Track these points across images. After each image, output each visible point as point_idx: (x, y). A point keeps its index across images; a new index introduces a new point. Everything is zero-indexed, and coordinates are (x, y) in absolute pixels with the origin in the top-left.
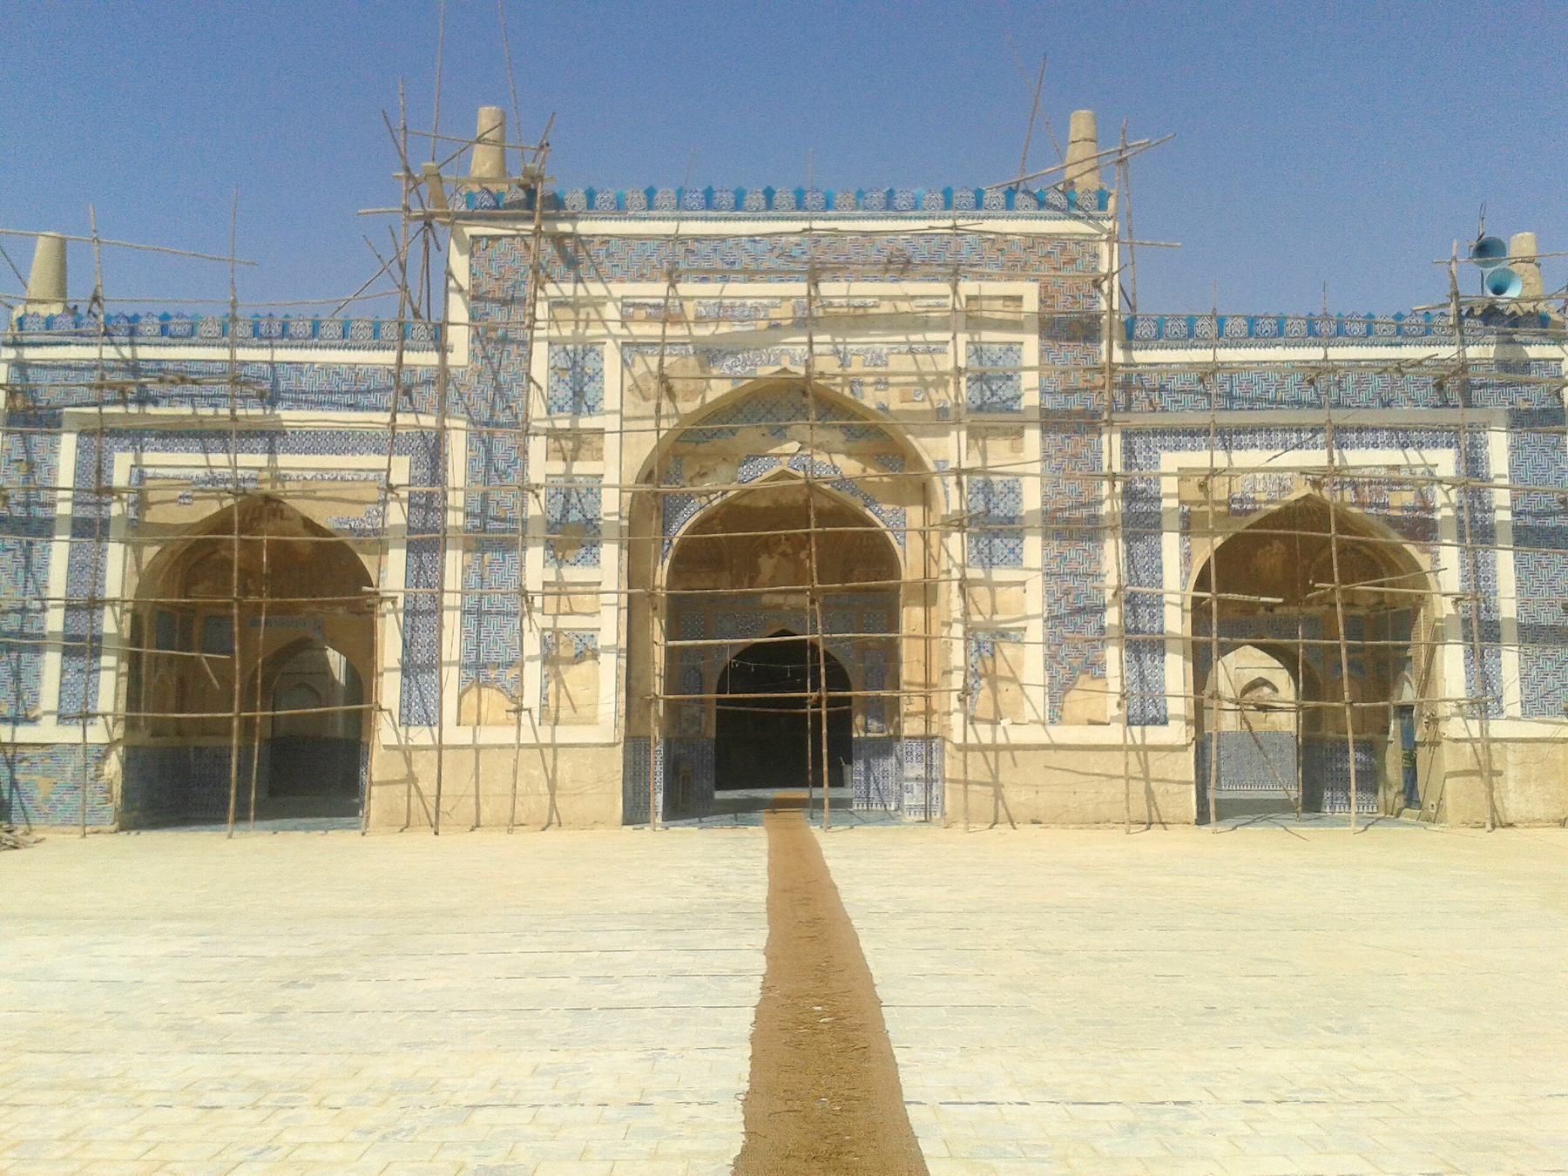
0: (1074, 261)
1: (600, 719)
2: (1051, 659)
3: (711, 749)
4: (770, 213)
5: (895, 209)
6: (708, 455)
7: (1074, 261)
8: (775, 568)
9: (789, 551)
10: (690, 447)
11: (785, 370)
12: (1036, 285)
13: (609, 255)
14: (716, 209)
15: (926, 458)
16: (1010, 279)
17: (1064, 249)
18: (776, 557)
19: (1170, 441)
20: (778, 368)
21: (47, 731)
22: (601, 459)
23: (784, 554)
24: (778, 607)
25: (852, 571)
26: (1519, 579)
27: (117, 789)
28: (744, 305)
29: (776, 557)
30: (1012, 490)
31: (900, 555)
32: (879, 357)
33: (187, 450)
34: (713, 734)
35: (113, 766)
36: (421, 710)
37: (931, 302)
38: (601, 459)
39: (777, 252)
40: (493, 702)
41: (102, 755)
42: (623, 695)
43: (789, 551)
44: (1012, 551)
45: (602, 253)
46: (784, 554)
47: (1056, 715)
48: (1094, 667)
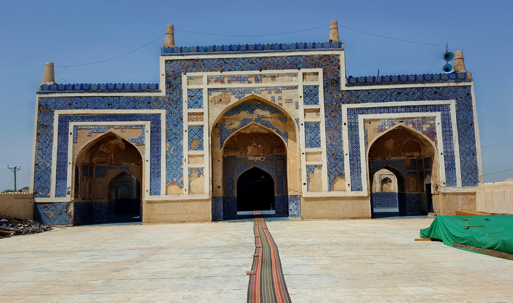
0: (333, 62)
2: (329, 173)
3: (236, 200)
6: (233, 119)
7: (333, 62)
8: (252, 150)
10: (227, 117)
13: (203, 64)
15: (293, 118)
17: (329, 59)
19: (361, 111)
21: (52, 198)
22: (203, 121)
23: (254, 146)
26: (460, 148)
27: (72, 214)
30: (317, 126)
31: (286, 145)
32: (279, 90)
33: (89, 121)
35: (71, 209)
36: (155, 191)
38: (203, 121)
39: (250, 62)
40: (173, 188)
41: (68, 205)
42: (211, 185)
44: (317, 143)
45: (202, 64)
46: (254, 146)
47: (331, 188)
48: (342, 175)
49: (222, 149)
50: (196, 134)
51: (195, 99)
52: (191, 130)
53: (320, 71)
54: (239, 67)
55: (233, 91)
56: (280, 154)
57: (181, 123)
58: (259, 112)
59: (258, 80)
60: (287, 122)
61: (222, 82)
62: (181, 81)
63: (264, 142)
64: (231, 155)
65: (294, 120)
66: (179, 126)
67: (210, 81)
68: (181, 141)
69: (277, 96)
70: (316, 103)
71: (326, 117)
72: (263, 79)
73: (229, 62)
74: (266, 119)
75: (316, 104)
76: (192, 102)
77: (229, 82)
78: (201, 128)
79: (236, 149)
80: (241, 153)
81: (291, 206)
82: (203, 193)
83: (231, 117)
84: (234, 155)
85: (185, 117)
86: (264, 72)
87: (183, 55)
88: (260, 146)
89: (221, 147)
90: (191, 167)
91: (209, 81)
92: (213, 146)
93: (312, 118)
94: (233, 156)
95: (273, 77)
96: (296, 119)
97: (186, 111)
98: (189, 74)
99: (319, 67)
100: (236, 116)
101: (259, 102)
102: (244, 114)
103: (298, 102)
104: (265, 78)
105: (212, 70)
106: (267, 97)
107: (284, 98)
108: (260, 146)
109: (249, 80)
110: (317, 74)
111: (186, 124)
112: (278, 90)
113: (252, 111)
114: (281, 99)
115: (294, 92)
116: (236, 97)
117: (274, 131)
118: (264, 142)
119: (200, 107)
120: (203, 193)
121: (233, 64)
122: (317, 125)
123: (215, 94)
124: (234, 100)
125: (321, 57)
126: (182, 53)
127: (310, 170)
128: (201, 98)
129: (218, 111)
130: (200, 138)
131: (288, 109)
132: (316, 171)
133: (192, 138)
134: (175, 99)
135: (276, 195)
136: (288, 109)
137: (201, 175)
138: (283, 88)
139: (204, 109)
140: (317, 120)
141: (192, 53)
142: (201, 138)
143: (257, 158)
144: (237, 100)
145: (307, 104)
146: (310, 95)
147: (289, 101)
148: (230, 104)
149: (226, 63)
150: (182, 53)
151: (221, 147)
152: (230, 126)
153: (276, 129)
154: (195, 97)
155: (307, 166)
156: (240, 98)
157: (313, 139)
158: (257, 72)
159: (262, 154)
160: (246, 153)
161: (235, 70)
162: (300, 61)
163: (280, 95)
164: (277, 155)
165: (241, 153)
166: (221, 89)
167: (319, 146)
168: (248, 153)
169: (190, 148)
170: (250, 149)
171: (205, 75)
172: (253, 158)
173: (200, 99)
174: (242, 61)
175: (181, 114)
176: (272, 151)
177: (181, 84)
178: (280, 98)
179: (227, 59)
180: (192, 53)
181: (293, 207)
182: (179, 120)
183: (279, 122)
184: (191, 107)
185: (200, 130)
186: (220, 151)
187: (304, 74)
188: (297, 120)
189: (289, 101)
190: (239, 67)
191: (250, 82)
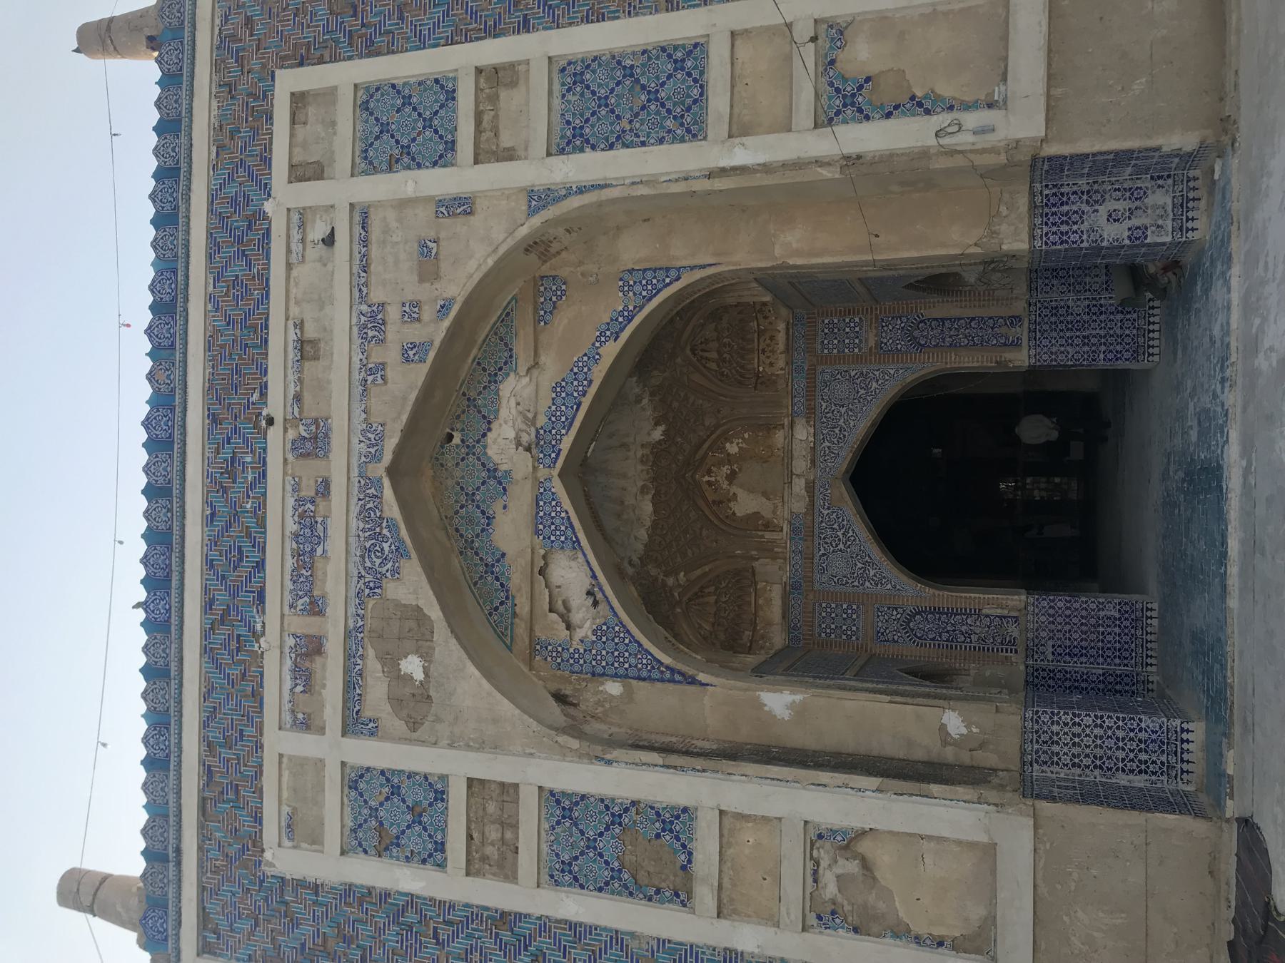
0: (249, 20)
1: (983, 838)
4: (175, 492)
5: (175, 299)
9: (725, 470)
10: (521, 630)
11: (392, 471)
12: (278, 72)
13: (228, 744)
14: (169, 575)
15: (523, 231)
16: (270, 117)
17: (233, 38)
18: (734, 489)
20: (386, 482)
22: (516, 786)
23: (731, 477)
24: (810, 487)
25: (757, 375)
28: (296, 536)
29: (734, 489)
31: (698, 274)
32: (372, 317)
34: (1016, 600)
37: (294, 232)
39: (227, 482)
43: (725, 470)
44: (679, 65)
46: (731, 477)
49: (702, 677)
50: (591, 845)
51: (395, 816)
52: (566, 867)
53: (288, 81)
54: (246, 546)
55: (370, 586)
56: (781, 338)
57: (524, 928)
58: (503, 443)
59: (312, 444)
60: (564, 272)
61: (311, 648)
62: (300, 884)
63: (709, 421)
64: (775, 611)
65: (536, 221)
66: (543, 942)
67: (308, 716)
68: (633, 945)
69: (397, 333)
70: (445, 89)
71: (525, 26)
72: (311, 410)
73: (222, 597)
74: (545, 403)
75: (451, 95)
76: (413, 840)
77: (316, 608)
78: (563, 807)
79: (743, 581)
80: (768, 551)
81: (1106, 226)
82: (988, 852)
83: (523, 607)
84: (776, 594)
85: (488, 893)
86: (276, 405)
87: (178, 851)
88: (732, 448)
89: (692, 681)
90: (796, 913)
91: (306, 724)
92: (676, 750)
93: (534, 108)
94: (785, 597)
95: (307, 350)
96: (532, 212)
97: (450, 885)
98: (270, 831)
99: (267, 95)
100: (517, 580)
101: (450, 437)
102: (511, 531)
103: (440, 203)
104: (307, 397)
105: (257, 696)
106: (406, 382)
107: (414, 290)
108: (732, 448)
109: (308, 492)
110: (299, 100)
111: (528, 896)
112: (372, 324)
113: (498, 479)
114: (416, 304)
115: (386, 231)
116: (396, 571)
117: (611, 350)
118: (709, 421)
119: (441, 796)
120: (988, 852)
121: (232, 576)
122: (574, 74)
123: (376, 692)
124: (411, 587)
125: (226, 89)
126: (172, 855)
127: (849, 101)
128: (393, 782)
129: (469, 688)
130: (616, 819)
131: (473, 255)
132: (862, 56)
133: (616, 874)
134: (391, 936)
135: (1021, 359)
136: (472, 264)
137: (864, 847)
138: (360, 289)
139: (456, 766)
140: (539, 79)
141: (172, 798)
142: (618, 814)
143: (800, 465)
144: (413, 570)
145: (451, 146)
146: (405, 130)
147: (428, 260)
148: (435, 613)
149: (227, 611)
150: (172, 855)
151: (692, 681)
152: (576, 617)
153: (602, 338)
154: (395, 813)
155: (825, 120)
156: (400, 551)
157: (653, 96)
158: (275, 437)
159: (779, 437)
160: (768, 526)
161: (260, 565)
162: (233, 201)
163: (393, 313)
164: (787, 350)
165: (768, 551)
166: (348, 656)
167: (697, 49)
168: (767, 514)
169: (682, 896)
170: (746, 504)
171: (279, 742)
172: (799, 486)
173: (396, 790)
174: (219, 524)
175: (475, 915)
176: (761, 381)
177: (316, 888)
178: (412, 312)
179: (208, 606)
180: (172, 798)
181: (1112, 218)
182: (506, 935)
183: (562, 321)
184: (441, 847)
185: (567, 814)
186: (717, 699)
187: (303, 172)
188: (538, 198)
189: (428, 260)
190: (246, 546)
191: (324, 488)
